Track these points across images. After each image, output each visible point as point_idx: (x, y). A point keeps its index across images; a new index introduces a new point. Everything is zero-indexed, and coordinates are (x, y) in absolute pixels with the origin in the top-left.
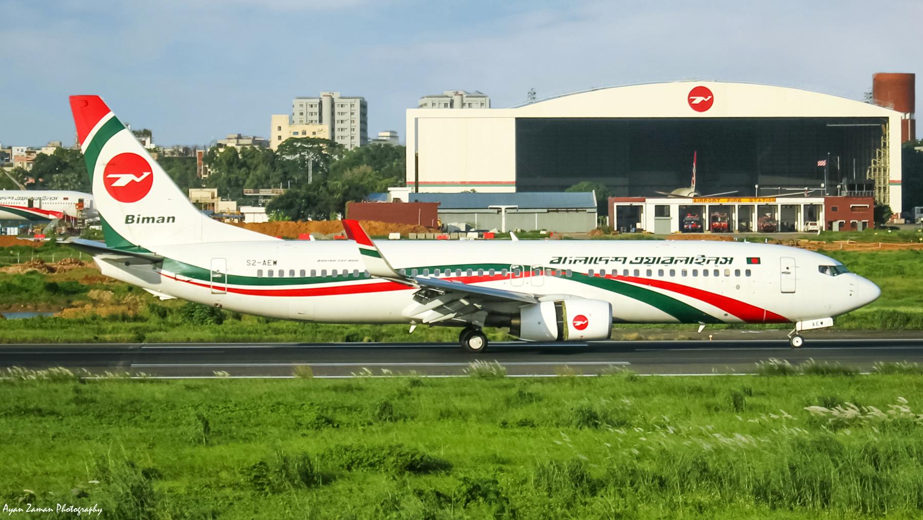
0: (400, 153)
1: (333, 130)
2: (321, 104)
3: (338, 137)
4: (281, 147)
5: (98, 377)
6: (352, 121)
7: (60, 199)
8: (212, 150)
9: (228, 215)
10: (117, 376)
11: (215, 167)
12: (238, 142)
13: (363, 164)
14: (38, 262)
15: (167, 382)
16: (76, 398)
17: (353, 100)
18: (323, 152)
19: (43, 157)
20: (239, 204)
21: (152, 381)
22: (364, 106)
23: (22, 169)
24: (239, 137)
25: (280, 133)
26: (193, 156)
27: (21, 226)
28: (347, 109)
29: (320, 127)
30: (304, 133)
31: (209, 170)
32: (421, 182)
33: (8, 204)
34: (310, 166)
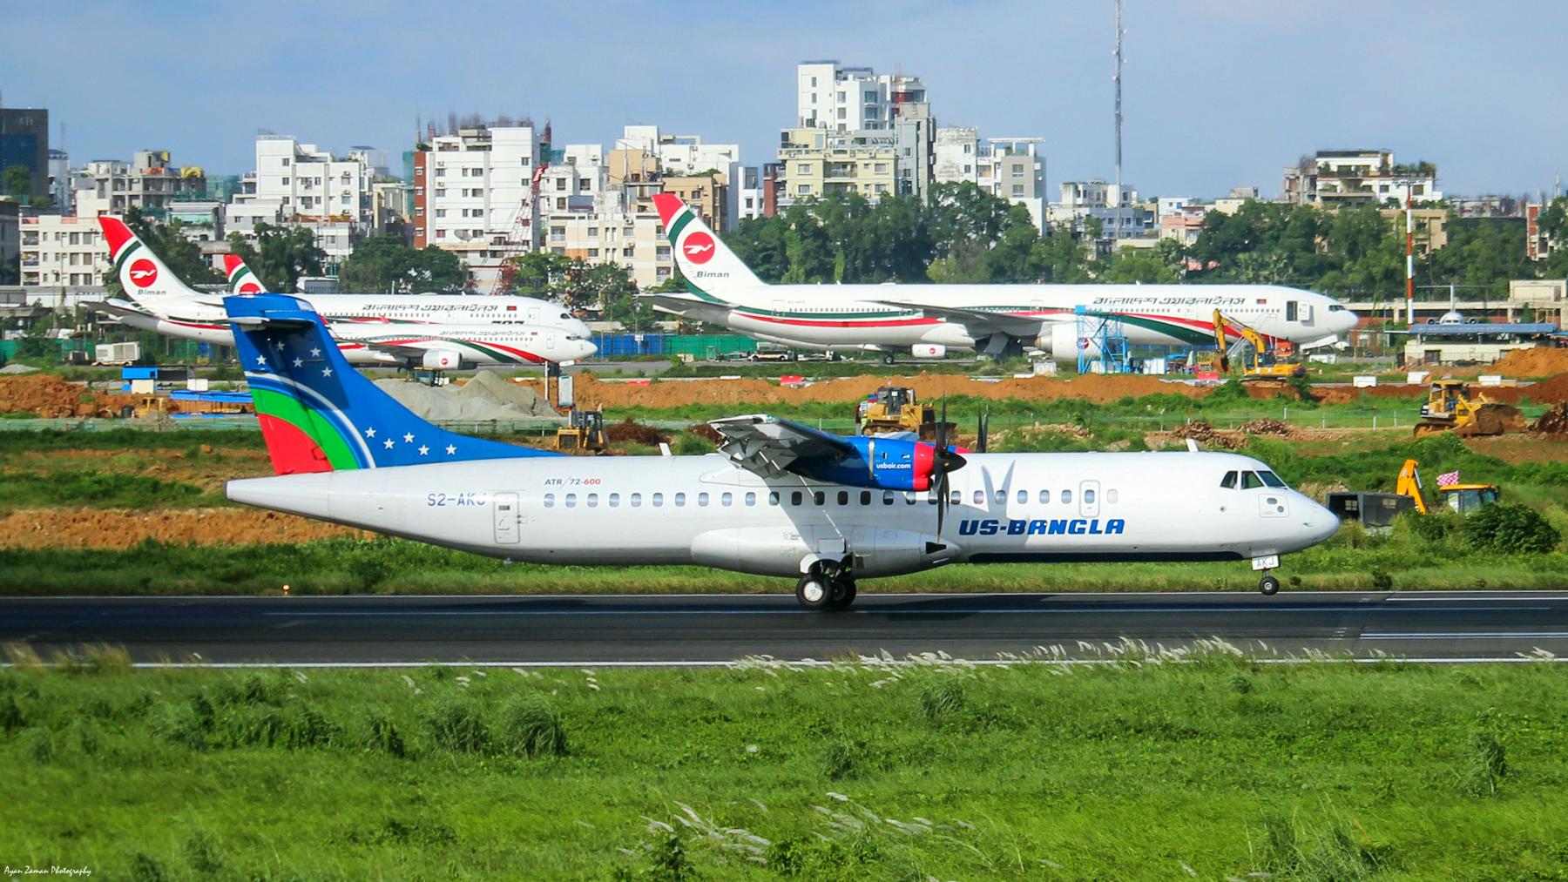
5: (1294, 660)
7: (1251, 303)
8: (1555, 203)
11: (1563, 236)
14: (1199, 427)
16: (1242, 702)
19: (1217, 220)
21: (1400, 668)
26: (1520, 215)
27: (1172, 357)
31: (1550, 243)
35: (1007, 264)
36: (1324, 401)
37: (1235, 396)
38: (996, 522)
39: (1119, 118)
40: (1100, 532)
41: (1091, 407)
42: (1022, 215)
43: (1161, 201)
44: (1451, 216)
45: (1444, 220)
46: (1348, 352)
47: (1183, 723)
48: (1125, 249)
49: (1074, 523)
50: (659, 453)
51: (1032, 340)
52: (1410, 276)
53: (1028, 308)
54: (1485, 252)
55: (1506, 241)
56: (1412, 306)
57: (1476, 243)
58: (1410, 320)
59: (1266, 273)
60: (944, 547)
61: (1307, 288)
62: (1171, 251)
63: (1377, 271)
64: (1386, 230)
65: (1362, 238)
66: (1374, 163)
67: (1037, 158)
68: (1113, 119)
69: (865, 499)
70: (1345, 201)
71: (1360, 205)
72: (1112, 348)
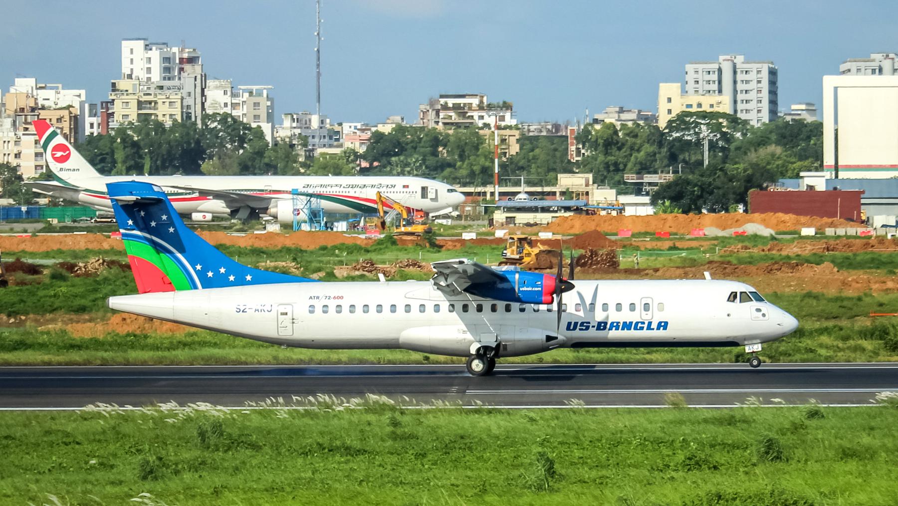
0: (817, 130)
1: (735, 102)
2: (720, 70)
3: (742, 111)
4: (670, 122)
5: (425, 407)
6: (759, 91)
7: (399, 188)
8: (585, 127)
9: (605, 206)
10: (448, 406)
11: (590, 147)
12: (619, 116)
13: (770, 144)
14: (367, 264)
15: (508, 413)
16: (393, 433)
17: (759, 65)
18: (724, 130)
19: (378, 137)
20: (619, 193)
21: (490, 412)
22: (773, 73)
23: (354, 150)
24: (621, 111)
25: (669, 106)
26: (564, 134)
27: (351, 220)
28: (752, 76)
29: (718, 98)
30: (700, 105)
31: (583, 151)
32: (842, 166)
33: (334, 193)
34: (706, 147)
35: (250, 164)
36: (444, 248)
37: (389, 244)
38: (589, 323)
39: (319, 74)
40: (653, 329)
41: (301, 251)
42: (259, 134)
43: (344, 125)
44: (522, 134)
45: (518, 137)
46: (459, 217)
47: (357, 445)
48: (323, 154)
49: (637, 323)
50: (378, 280)
51: (265, 210)
52: (496, 171)
53: (262, 190)
54: (543, 157)
55: (556, 150)
56: (498, 189)
57: (537, 151)
58: (497, 199)
59: (408, 169)
60: (556, 338)
61: (434, 178)
62: (352, 155)
63: (477, 168)
64: (482, 143)
65: (467, 149)
66: (475, 102)
67: (268, 98)
68: (315, 74)
69: (508, 309)
70: (458, 125)
71: (466, 127)
72: (314, 216)
